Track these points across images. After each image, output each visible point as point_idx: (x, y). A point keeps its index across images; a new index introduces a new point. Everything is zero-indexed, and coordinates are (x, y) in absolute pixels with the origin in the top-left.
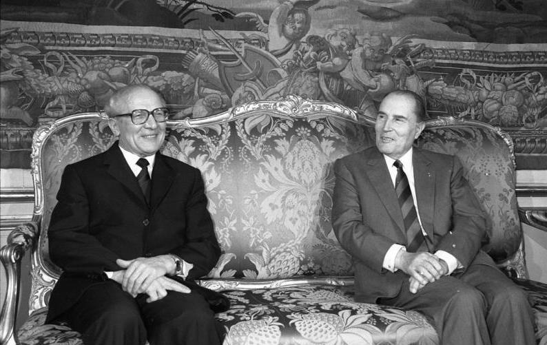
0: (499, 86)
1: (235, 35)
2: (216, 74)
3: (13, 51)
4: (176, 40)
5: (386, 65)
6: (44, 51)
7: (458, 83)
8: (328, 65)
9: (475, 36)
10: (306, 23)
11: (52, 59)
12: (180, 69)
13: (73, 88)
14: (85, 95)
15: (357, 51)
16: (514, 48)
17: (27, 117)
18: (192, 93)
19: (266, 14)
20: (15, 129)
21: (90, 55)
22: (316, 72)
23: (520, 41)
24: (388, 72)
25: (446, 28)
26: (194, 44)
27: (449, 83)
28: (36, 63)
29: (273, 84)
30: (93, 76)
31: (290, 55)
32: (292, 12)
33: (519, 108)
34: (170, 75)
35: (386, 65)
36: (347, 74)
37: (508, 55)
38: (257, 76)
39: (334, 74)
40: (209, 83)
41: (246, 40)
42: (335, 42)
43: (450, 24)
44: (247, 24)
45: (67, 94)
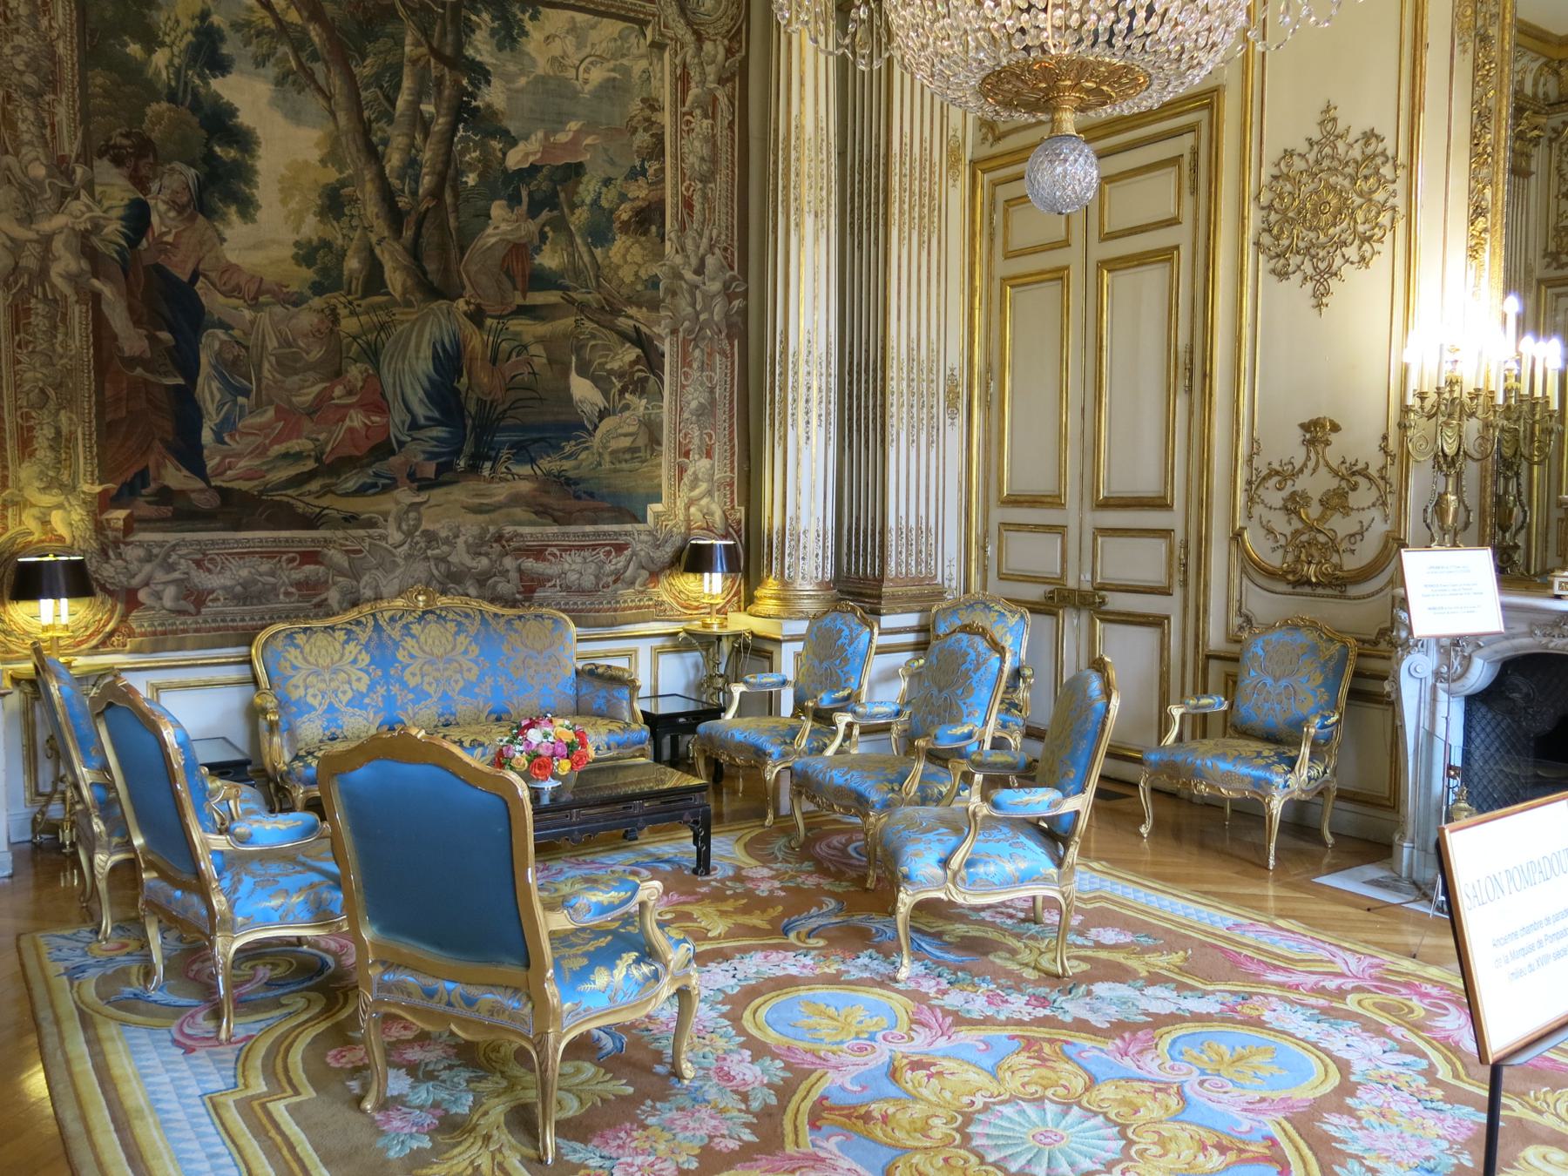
0: (579, 560)
1: (362, 532)
2: (346, 565)
3: (181, 557)
4: (313, 540)
5: (484, 549)
6: (205, 555)
7: (544, 560)
8: (437, 552)
9: (557, 521)
10: (419, 520)
11: (212, 560)
12: (317, 563)
13: (229, 583)
14: (239, 589)
15: (461, 541)
16: (589, 528)
17: (192, 608)
18: (326, 582)
19: (385, 515)
20: (183, 618)
21: (241, 555)
22: (427, 558)
23: (594, 522)
24: (487, 555)
25: (533, 517)
26: (327, 542)
27: (537, 560)
28: (198, 564)
29: (392, 571)
30: (244, 573)
31: (406, 547)
32: (407, 512)
33: (597, 577)
34: (309, 568)
35: (484, 549)
36: (453, 559)
37: (585, 535)
38: (380, 566)
39: (442, 559)
40: (341, 573)
41: (370, 537)
42: (443, 534)
43: (536, 513)
44: (371, 524)
45: (224, 588)
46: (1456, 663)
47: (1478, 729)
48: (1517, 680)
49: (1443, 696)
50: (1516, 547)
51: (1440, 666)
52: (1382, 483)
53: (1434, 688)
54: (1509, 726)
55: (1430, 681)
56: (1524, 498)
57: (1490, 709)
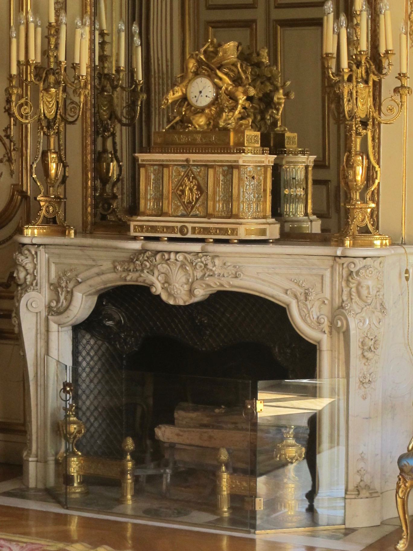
46: (62, 298)
47: (84, 353)
48: (111, 309)
49: (54, 327)
50: (115, 197)
51: (51, 301)
52: (7, 141)
53: (47, 320)
54: (107, 349)
55: (44, 314)
56: (119, 154)
57: (93, 336)
